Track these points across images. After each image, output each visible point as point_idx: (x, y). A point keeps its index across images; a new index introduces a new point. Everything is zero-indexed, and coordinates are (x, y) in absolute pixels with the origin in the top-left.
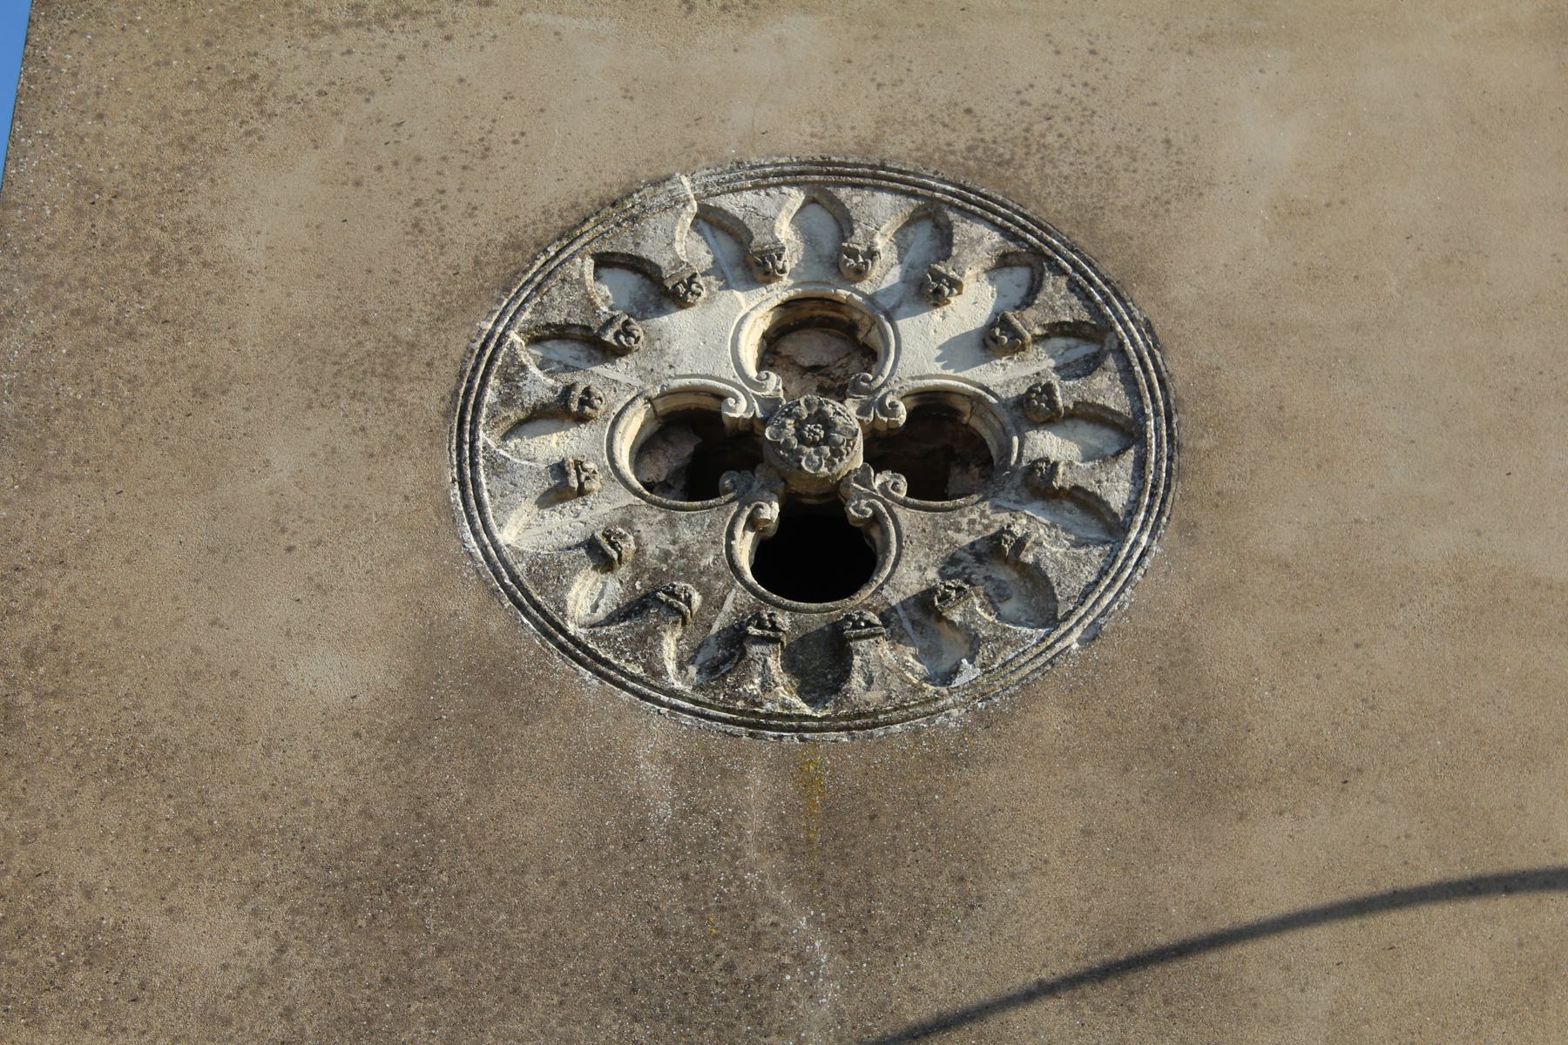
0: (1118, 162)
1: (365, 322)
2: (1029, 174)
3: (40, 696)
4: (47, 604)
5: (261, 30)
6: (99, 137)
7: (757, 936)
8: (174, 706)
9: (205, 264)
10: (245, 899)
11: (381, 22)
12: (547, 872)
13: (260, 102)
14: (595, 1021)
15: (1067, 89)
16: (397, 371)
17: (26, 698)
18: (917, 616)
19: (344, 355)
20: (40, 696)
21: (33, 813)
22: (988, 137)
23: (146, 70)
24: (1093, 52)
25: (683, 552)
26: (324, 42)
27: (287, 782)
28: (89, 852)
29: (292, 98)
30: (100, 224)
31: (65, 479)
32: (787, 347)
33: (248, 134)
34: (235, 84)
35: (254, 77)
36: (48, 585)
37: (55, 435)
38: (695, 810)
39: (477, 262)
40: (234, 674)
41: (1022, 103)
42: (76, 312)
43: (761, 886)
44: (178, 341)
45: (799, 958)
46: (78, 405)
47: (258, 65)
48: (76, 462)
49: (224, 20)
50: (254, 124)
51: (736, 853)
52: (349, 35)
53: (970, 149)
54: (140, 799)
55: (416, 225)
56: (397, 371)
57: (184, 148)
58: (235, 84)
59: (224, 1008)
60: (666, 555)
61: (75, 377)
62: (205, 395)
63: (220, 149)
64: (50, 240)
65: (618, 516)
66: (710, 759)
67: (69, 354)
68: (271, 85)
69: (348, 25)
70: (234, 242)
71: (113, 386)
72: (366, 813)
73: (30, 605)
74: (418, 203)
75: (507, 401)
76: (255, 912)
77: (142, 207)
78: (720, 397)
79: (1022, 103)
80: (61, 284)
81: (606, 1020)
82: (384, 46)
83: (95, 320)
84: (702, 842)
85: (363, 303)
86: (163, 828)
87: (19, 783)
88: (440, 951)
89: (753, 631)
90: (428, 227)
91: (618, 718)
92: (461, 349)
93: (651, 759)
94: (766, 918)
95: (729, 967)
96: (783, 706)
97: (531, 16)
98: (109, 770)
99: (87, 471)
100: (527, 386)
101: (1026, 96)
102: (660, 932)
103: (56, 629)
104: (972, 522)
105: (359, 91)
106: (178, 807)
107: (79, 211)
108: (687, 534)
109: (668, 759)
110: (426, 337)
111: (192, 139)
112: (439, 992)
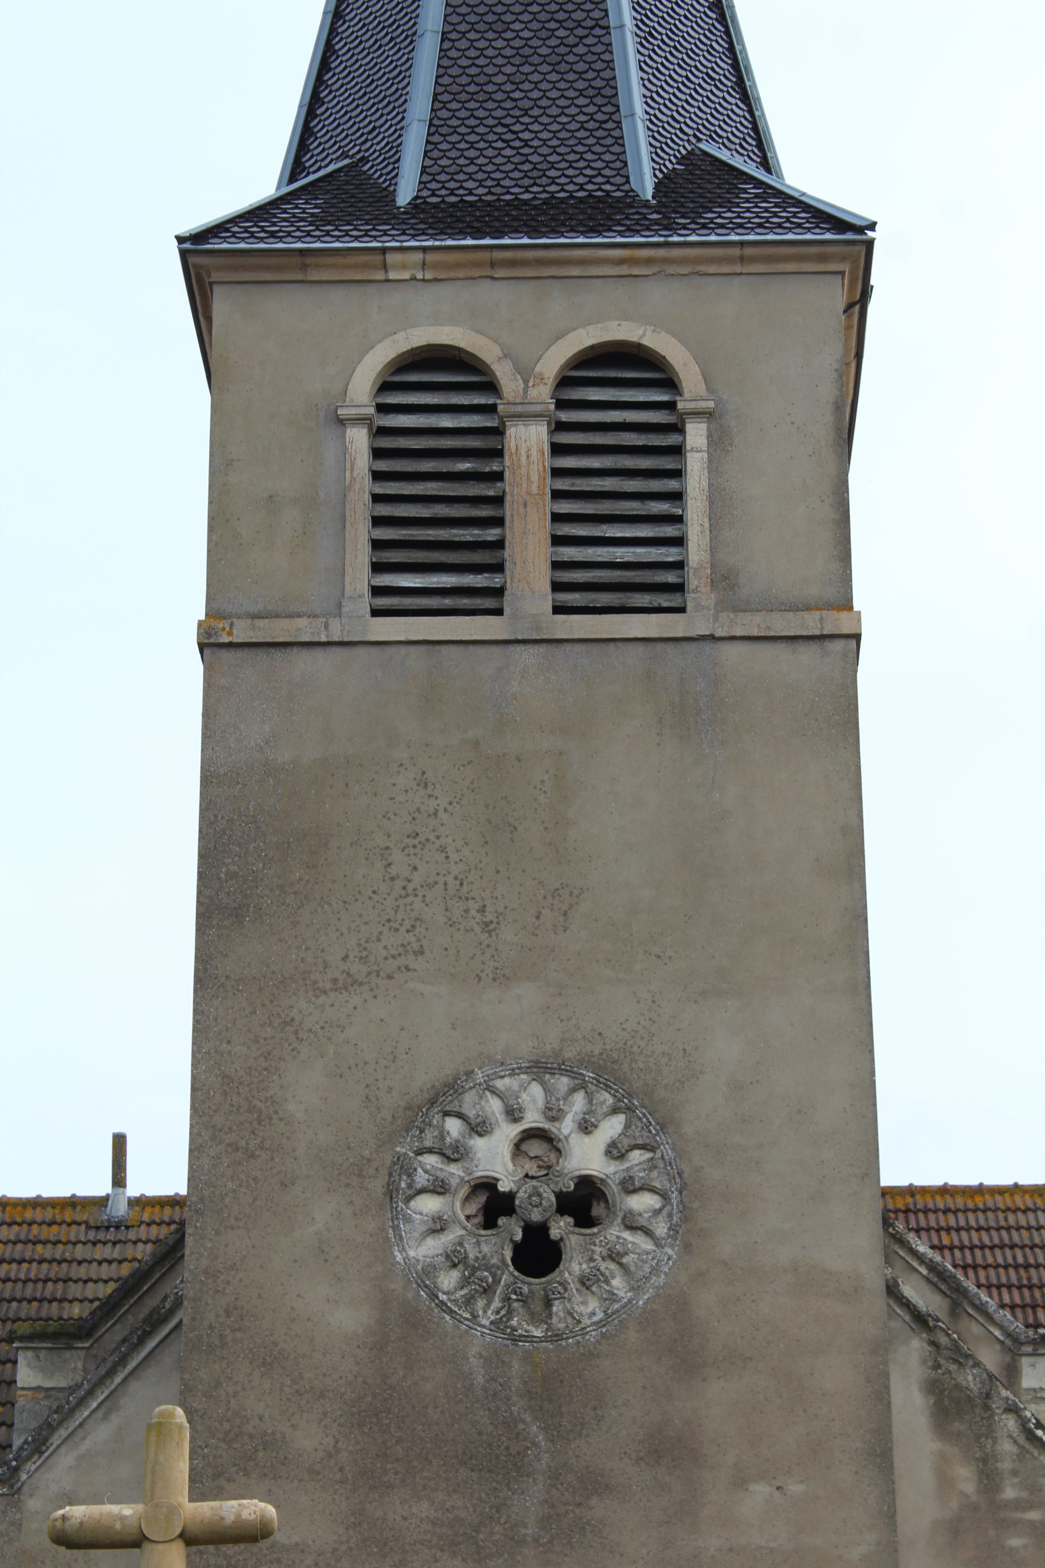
0: (663, 1061)
1: (349, 1148)
2: (626, 1067)
3: (234, 1330)
4: (231, 1288)
5: (294, 994)
6: (229, 1052)
7: (518, 1434)
8: (286, 1334)
9: (280, 1119)
10: (321, 1421)
11: (346, 988)
12: (436, 1407)
13: (296, 1033)
14: (457, 1471)
15: (642, 1022)
16: (364, 1173)
17: (227, 1332)
18: (579, 1286)
19: (341, 1165)
20: (234, 1330)
21: (236, 1383)
22: (608, 1047)
23: (246, 1016)
24: (654, 1002)
25: (484, 1257)
26: (322, 1000)
27: (333, 1368)
28: (259, 1400)
29: (310, 1030)
30: (234, 1099)
31: (232, 1228)
32: (524, 1147)
33: (293, 1050)
34: (285, 1023)
35: (293, 1020)
36: (231, 1279)
37: (226, 1206)
38: (492, 1379)
39: (394, 1117)
40: (309, 1319)
41: (623, 1029)
42: (229, 1145)
43: (519, 1413)
44: (272, 1159)
45: (534, 1444)
46: (234, 1191)
47: (294, 1013)
48: (236, 1219)
49: (278, 988)
50: (295, 1045)
51: (509, 1398)
52: (332, 995)
53: (601, 1054)
54: (276, 1377)
55: (367, 1098)
56: (364, 1173)
57: (266, 1058)
58: (285, 1023)
59: (318, 1467)
60: (477, 1258)
61: (232, 1177)
62: (286, 1186)
63: (281, 1059)
64: (213, 1107)
65: (457, 1240)
66: (497, 1356)
67: (228, 1166)
68: (301, 1023)
69: (331, 990)
70: (291, 1107)
71: (248, 1182)
72: (364, 1382)
73: (224, 1289)
74: (367, 1086)
75: (410, 1186)
76: (325, 1426)
77: (251, 1090)
78: (497, 1180)
79: (623, 1029)
80: (221, 1130)
81: (461, 1471)
82: (347, 1002)
83: (237, 1149)
84: (495, 1394)
85: (347, 1138)
86: (287, 1390)
87: (229, 1370)
88: (397, 1442)
89: (514, 1297)
90: (373, 1099)
91: (461, 1338)
92: (389, 1162)
93: (474, 1356)
94: (521, 1426)
95: (507, 1448)
96: (526, 1331)
97: (411, 985)
98: (264, 1364)
99: (241, 1224)
100: (417, 1179)
101: (624, 1026)
102: (480, 1434)
103: (236, 1299)
104: (601, 1241)
105: (339, 1026)
106: (292, 1380)
107: (225, 1093)
108: (486, 1249)
109: (481, 1356)
110: (375, 1156)
111: (269, 1054)
112: (398, 1460)
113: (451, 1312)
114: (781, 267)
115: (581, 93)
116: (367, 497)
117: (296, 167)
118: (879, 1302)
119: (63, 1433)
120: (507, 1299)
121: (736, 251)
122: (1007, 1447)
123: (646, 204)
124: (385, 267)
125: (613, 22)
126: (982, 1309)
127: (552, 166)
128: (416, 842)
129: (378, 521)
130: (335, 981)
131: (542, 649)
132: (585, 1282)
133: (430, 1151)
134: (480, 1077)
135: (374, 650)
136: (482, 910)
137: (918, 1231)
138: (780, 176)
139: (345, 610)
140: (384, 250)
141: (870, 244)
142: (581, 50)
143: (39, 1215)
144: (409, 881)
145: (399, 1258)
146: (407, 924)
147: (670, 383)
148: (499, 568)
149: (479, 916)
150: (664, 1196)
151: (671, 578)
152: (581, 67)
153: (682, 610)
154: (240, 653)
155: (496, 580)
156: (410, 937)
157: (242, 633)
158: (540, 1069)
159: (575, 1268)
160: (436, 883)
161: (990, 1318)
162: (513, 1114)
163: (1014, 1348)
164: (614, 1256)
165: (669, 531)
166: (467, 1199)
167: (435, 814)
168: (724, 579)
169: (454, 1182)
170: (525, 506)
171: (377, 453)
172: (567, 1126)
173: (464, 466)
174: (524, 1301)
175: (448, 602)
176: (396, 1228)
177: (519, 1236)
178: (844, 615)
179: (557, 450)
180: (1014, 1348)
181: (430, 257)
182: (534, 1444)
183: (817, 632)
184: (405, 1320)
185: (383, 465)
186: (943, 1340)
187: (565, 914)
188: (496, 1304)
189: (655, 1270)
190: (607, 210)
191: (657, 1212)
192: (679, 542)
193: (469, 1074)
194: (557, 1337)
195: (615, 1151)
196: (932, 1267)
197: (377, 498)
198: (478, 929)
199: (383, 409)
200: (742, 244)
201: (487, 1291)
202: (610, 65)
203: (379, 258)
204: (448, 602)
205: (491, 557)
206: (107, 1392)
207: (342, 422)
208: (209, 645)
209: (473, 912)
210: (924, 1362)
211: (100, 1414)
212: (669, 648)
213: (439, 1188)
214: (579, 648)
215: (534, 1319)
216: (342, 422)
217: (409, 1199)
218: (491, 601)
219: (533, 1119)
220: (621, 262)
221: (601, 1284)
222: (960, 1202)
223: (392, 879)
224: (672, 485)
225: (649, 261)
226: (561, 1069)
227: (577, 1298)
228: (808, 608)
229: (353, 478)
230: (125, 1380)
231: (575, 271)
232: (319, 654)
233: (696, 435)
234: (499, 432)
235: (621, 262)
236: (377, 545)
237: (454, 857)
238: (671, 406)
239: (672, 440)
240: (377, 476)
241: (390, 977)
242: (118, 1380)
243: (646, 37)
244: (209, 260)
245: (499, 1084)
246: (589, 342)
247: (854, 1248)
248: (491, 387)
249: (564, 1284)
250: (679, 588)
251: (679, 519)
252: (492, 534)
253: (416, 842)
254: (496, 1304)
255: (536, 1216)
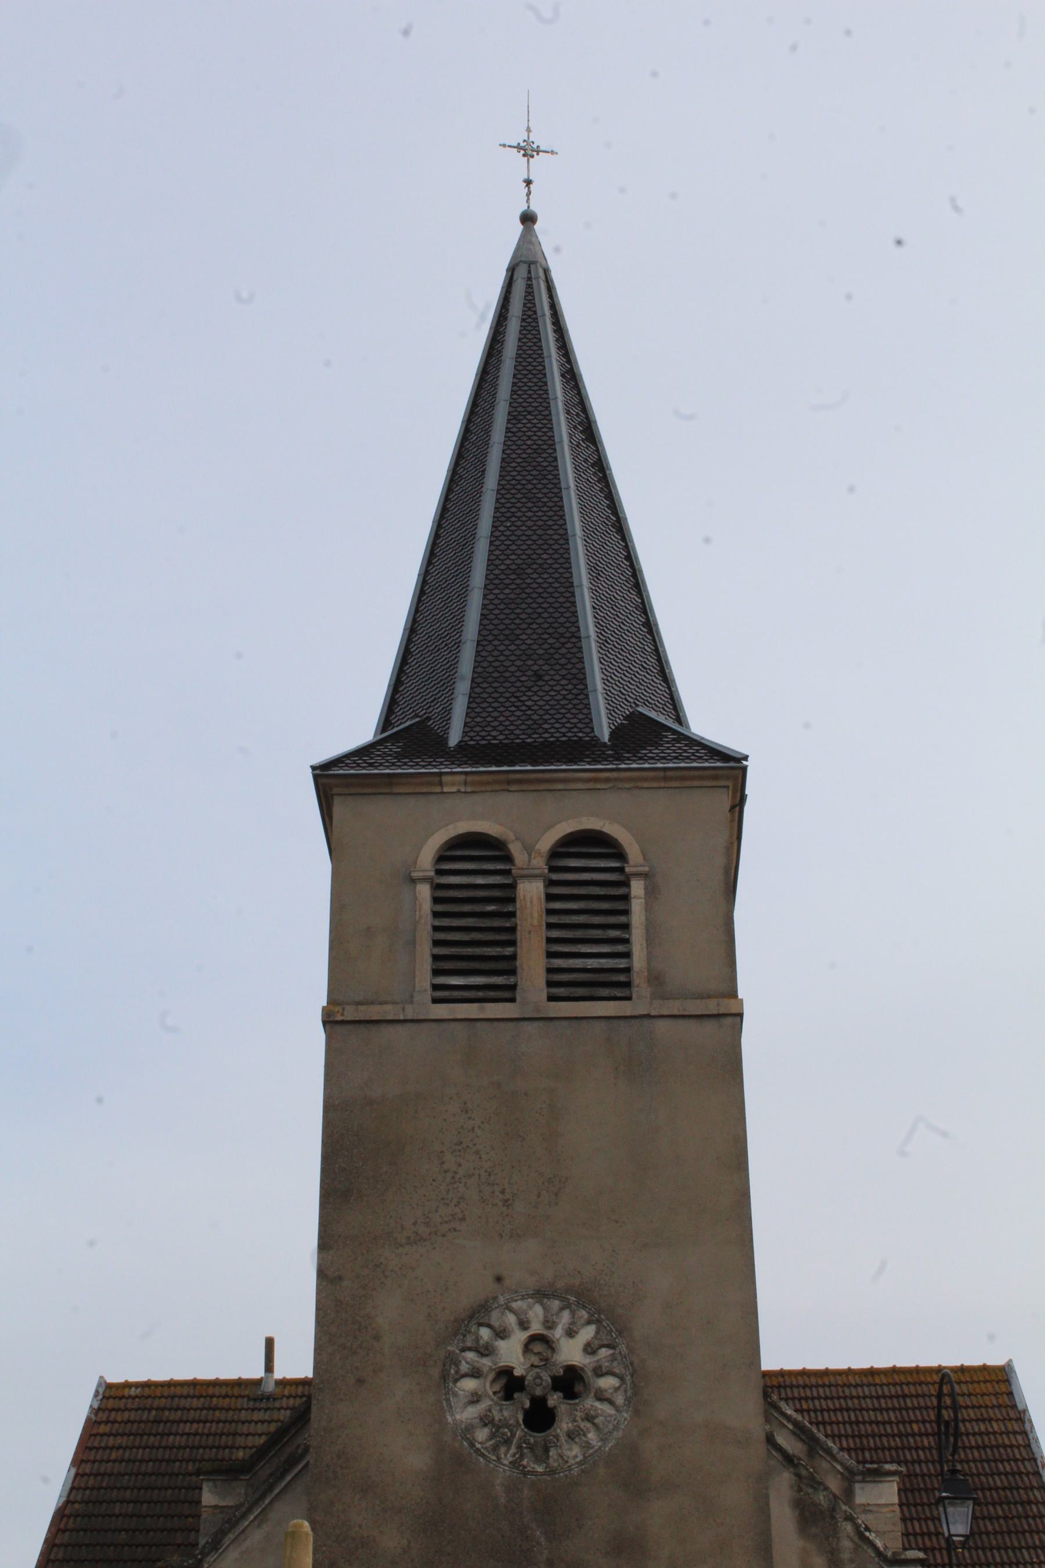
11: (415, 1242)
13: (383, 1272)
17: (338, 1469)
31: (342, 1400)
32: (531, 1347)
60: (500, 1420)
75: (457, 1372)
78: (513, 1368)
94: (529, 1532)
95: (520, 1546)
102: (503, 1537)
108: (506, 1413)
113: (483, 1455)
114: (688, 783)
115: (564, 677)
116: (429, 928)
117: (386, 722)
118: (760, 1448)
119: (231, 1536)
120: (519, 1447)
121: (661, 774)
122: (846, 1544)
123: (604, 745)
124: (441, 784)
125: (583, 634)
126: (828, 1451)
127: (546, 722)
128: (460, 1148)
129: (436, 943)
130: (408, 1238)
131: (541, 1024)
132: (571, 1436)
133: (470, 1349)
134: (502, 1300)
135: (434, 1025)
136: (503, 1192)
137: (786, 1400)
138: (688, 727)
139: (415, 999)
140: (440, 774)
141: (744, 769)
142: (563, 651)
143: (217, 1391)
144: (456, 1173)
145: (450, 1419)
146: (455, 1201)
147: (620, 855)
148: (513, 972)
149: (501, 1196)
150: (621, 1378)
151: (622, 978)
152: (563, 661)
153: (629, 998)
154: (350, 1027)
155: (512, 980)
156: (457, 1210)
157: (350, 1014)
158: (541, 1295)
159: (565, 1426)
160: (473, 1175)
161: (834, 1457)
162: (523, 1325)
163: (850, 1478)
164: (589, 1418)
165: (620, 948)
166: (494, 1381)
167: (473, 1130)
168: (656, 979)
169: (485, 1370)
170: (530, 933)
171: (436, 900)
172: (558, 1332)
173: (491, 908)
174: (531, 1448)
175: (481, 994)
176: (448, 1400)
177: (527, 1405)
178: (732, 1001)
179: (550, 898)
180: (850, 1478)
181: (470, 778)
182: (539, 1544)
183: (716, 1012)
184: (453, 1462)
185: (440, 908)
186: (804, 1473)
187: (556, 1195)
188: (513, 1450)
189: (616, 1428)
190: (581, 748)
191: (617, 1389)
192: (627, 955)
193: (495, 1298)
194: (552, 1472)
195: (589, 1349)
196: (796, 1423)
197: (436, 929)
198: (500, 1204)
199: (440, 872)
200: (665, 769)
201: (507, 1442)
202: (581, 660)
203: (437, 779)
204: (481, 994)
205: (508, 965)
206: (260, 1510)
207: (413, 881)
208: (329, 1021)
209: (497, 1193)
210: (791, 1487)
211: (256, 1523)
212: (622, 1023)
213: (475, 1373)
214: (564, 1023)
215: (538, 1460)
216: (413, 881)
217: (456, 1381)
218: (508, 993)
219: (536, 1328)
220: (589, 780)
221: (580, 1439)
222: (813, 1381)
223: (446, 1172)
224: (623, 919)
225: (607, 780)
226: (553, 1295)
227: (566, 1446)
228: (709, 997)
229: (420, 917)
230: (271, 1502)
231: (560, 786)
232: (399, 1028)
233: (637, 888)
234: (513, 886)
235: (589, 780)
236: (436, 958)
237: (485, 1157)
238: (621, 870)
239: (621, 891)
240: (436, 915)
241: (444, 1235)
242: (267, 1501)
243: (603, 643)
244: (333, 781)
245: (514, 1305)
246: (570, 830)
247: (746, 1414)
248: (508, 858)
249: (557, 1437)
250: (628, 984)
251: (627, 941)
252: (509, 951)
253: (460, 1148)
254: (513, 1450)
255: (538, 1392)
